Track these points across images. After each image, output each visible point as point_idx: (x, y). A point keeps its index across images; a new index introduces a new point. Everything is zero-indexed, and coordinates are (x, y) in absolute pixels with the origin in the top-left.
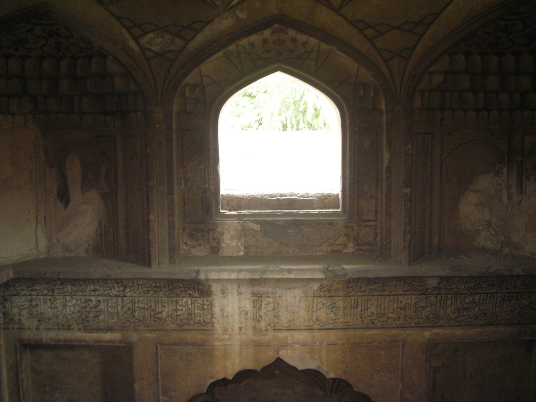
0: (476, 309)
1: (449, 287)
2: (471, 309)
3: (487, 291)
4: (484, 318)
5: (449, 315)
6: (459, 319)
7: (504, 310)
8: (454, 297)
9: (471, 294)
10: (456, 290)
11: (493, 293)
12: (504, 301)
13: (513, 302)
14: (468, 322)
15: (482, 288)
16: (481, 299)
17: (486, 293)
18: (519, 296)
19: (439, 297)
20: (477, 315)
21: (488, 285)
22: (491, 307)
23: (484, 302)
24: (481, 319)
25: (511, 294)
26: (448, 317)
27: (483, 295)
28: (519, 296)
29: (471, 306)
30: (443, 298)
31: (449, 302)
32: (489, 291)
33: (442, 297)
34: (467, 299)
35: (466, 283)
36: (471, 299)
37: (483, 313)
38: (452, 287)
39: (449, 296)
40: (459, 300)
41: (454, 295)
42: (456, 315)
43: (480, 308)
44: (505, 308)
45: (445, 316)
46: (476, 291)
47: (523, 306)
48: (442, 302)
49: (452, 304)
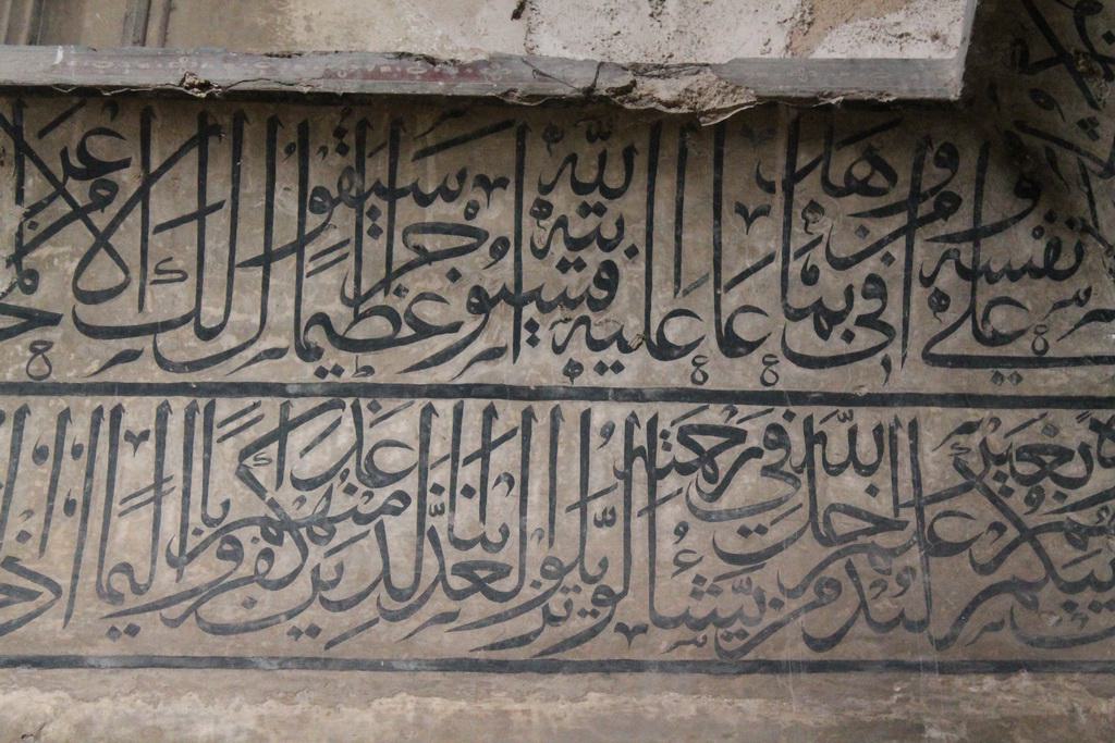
0: (400, 528)
1: (121, 311)
2: (346, 530)
3: (481, 373)
4: (477, 605)
5: (126, 568)
6: (225, 609)
7: (667, 547)
8: (176, 425)
9: (337, 395)
10: (183, 344)
11: (539, 394)
12: (655, 475)
13: (748, 484)
14: (314, 631)
15: (424, 331)
16: (438, 448)
17: (469, 391)
18: (796, 436)
19: (43, 411)
20: (402, 579)
21: (481, 303)
22: (536, 518)
23: (469, 474)
24: (446, 618)
25: (714, 415)
26: (120, 583)
27: (445, 406)
28: (796, 436)
29: (341, 504)
30: (78, 432)
31: (136, 465)
32: (503, 371)
33: (64, 417)
34: (298, 439)
35: (266, 261)
36: (344, 438)
37: (463, 569)
38: (156, 311)
39: (138, 413)
40: (226, 453)
41: (179, 404)
42: (201, 572)
43: (439, 523)
44: (682, 531)
45: (89, 578)
46: (388, 366)
47: (843, 524)
48: (72, 469)
49: (160, 480)
